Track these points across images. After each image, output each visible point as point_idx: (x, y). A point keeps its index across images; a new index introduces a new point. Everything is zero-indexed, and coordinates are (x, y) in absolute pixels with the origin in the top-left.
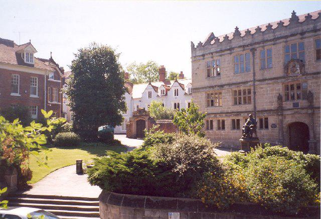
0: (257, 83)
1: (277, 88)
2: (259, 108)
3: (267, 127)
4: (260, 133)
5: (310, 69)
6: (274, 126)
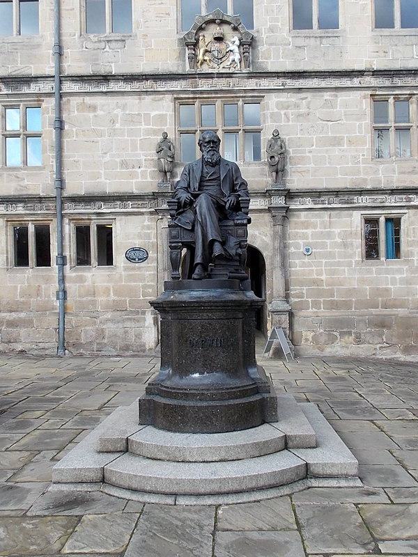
0: (68, 87)
1: (153, 114)
2: (75, 186)
3: (107, 257)
4: (81, 279)
5: (272, 57)
6: (137, 255)
